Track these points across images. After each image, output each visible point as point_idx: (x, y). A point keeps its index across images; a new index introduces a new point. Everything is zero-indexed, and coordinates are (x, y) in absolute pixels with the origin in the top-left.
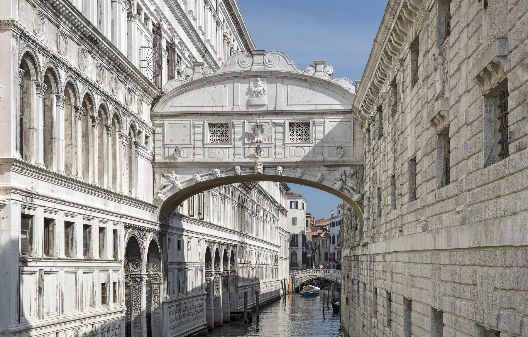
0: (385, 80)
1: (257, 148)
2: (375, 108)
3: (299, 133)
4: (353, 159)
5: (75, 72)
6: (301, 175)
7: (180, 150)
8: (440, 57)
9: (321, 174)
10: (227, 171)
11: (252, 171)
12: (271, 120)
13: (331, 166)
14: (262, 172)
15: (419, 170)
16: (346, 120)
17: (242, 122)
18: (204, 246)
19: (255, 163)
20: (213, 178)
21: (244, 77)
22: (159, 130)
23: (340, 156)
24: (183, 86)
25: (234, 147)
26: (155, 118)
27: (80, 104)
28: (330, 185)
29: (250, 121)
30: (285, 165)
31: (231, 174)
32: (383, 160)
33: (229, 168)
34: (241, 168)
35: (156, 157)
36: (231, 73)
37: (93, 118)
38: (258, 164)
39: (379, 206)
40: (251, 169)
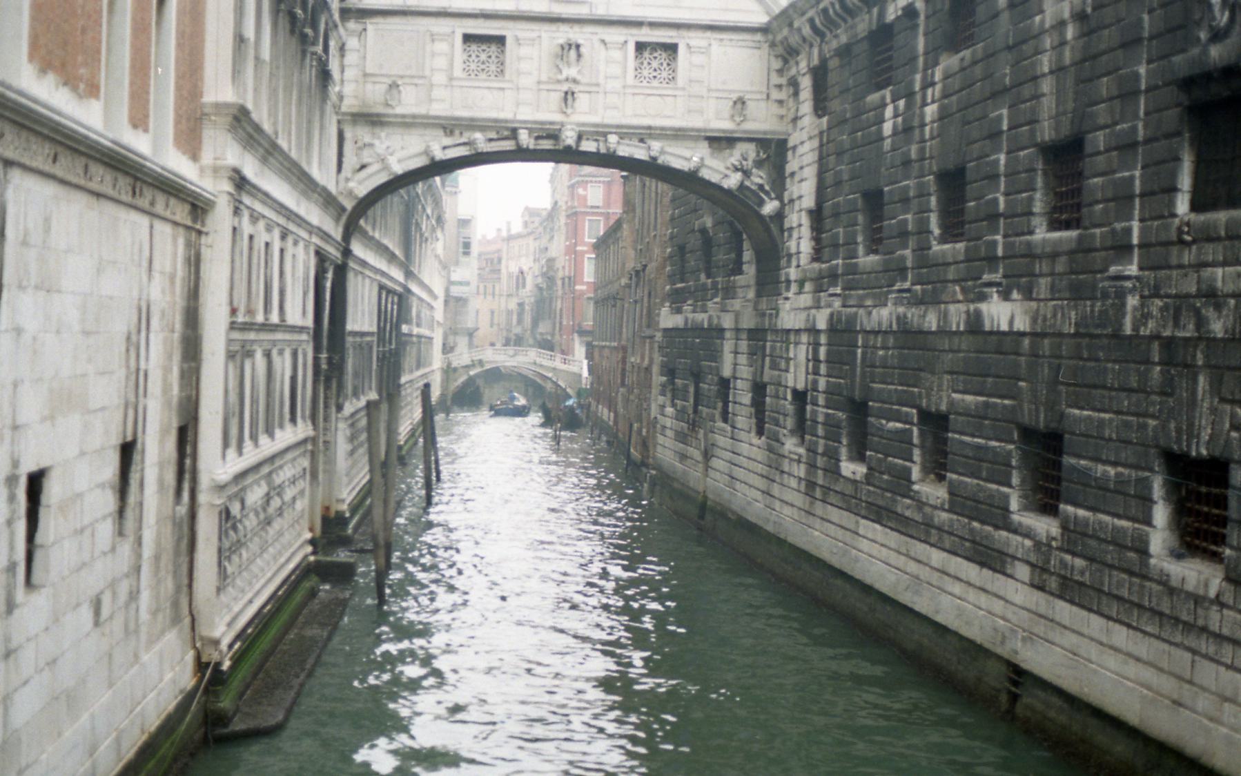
1: (566, 93)
3: (655, 64)
6: (657, 154)
7: (401, 88)
9: (699, 155)
10: (498, 139)
12: (596, 33)
13: (720, 142)
14: (574, 147)
16: (753, 45)
17: (534, 35)
18: (376, 289)
19: (562, 124)
20: (467, 153)
22: (352, 43)
23: (738, 119)
25: (518, 89)
28: (715, 178)
29: (557, 34)
30: (625, 132)
31: (508, 145)
34: (531, 130)
38: (569, 127)
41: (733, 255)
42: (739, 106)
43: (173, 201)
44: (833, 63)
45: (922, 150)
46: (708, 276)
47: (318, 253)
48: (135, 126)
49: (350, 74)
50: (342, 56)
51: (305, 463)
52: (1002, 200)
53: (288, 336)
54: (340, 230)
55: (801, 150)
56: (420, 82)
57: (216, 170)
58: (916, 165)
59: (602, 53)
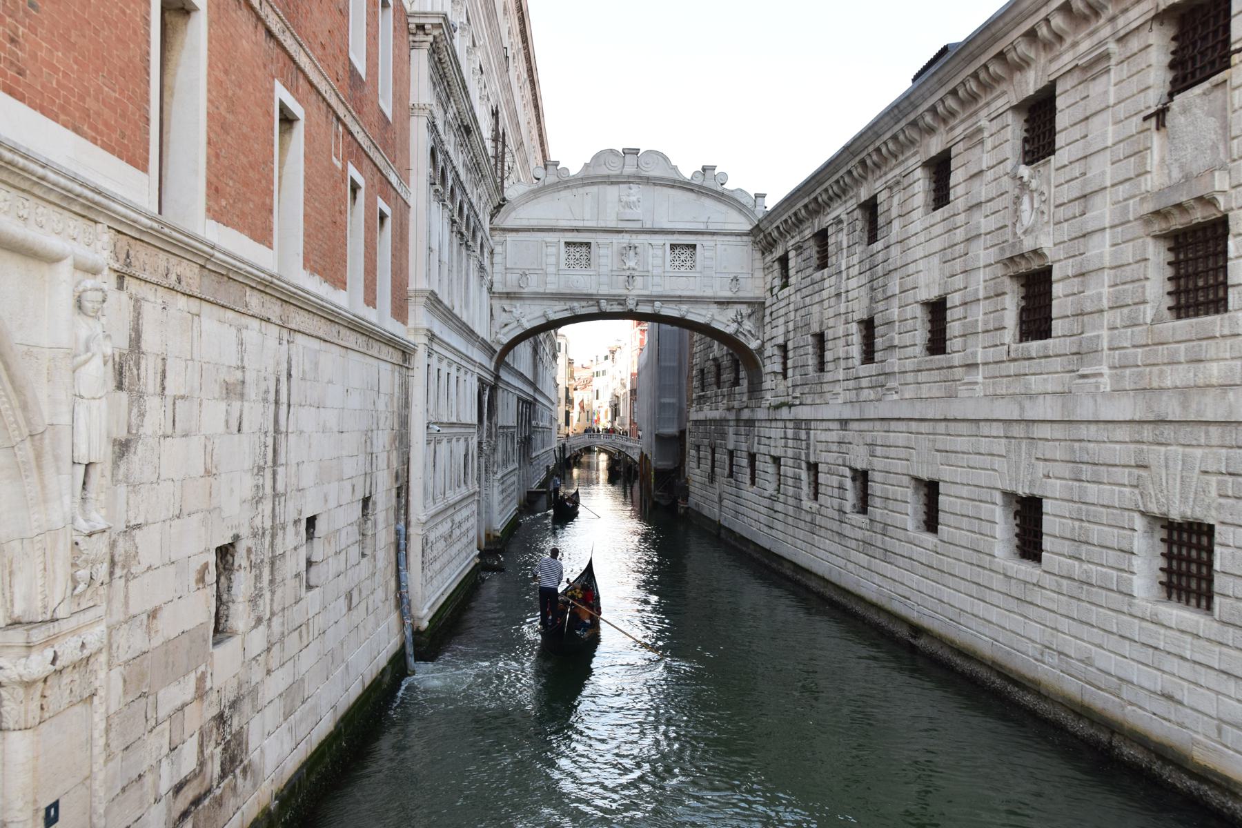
0: (839, 197)
2: (808, 233)
3: (682, 257)
4: (751, 295)
5: (456, 172)
8: (1033, 181)
11: (621, 307)
13: (723, 303)
15: (956, 317)
17: (608, 241)
21: (612, 183)
22: (498, 249)
23: (735, 290)
24: (533, 191)
26: (494, 233)
27: (456, 217)
31: (594, 310)
32: (832, 300)
33: (591, 303)
35: (495, 285)
36: (597, 177)
37: (462, 234)
39: (821, 357)
40: (619, 304)
41: (733, 375)
42: (734, 282)
43: (391, 350)
44: (792, 254)
45: (847, 307)
46: (719, 388)
47: (479, 379)
48: (368, 305)
49: (497, 268)
50: (492, 258)
51: (474, 507)
52: (896, 336)
53: (463, 430)
54: (493, 364)
55: (774, 308)
56: (541, 272)
57: (416, 330)
58: (843, 316)
59: (651, 251)
